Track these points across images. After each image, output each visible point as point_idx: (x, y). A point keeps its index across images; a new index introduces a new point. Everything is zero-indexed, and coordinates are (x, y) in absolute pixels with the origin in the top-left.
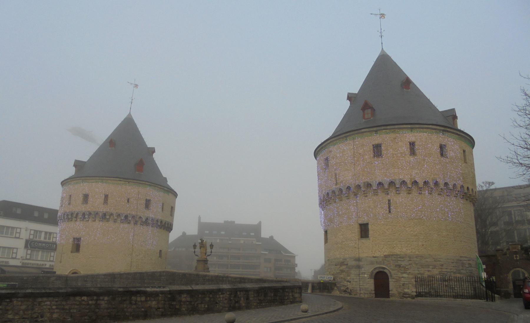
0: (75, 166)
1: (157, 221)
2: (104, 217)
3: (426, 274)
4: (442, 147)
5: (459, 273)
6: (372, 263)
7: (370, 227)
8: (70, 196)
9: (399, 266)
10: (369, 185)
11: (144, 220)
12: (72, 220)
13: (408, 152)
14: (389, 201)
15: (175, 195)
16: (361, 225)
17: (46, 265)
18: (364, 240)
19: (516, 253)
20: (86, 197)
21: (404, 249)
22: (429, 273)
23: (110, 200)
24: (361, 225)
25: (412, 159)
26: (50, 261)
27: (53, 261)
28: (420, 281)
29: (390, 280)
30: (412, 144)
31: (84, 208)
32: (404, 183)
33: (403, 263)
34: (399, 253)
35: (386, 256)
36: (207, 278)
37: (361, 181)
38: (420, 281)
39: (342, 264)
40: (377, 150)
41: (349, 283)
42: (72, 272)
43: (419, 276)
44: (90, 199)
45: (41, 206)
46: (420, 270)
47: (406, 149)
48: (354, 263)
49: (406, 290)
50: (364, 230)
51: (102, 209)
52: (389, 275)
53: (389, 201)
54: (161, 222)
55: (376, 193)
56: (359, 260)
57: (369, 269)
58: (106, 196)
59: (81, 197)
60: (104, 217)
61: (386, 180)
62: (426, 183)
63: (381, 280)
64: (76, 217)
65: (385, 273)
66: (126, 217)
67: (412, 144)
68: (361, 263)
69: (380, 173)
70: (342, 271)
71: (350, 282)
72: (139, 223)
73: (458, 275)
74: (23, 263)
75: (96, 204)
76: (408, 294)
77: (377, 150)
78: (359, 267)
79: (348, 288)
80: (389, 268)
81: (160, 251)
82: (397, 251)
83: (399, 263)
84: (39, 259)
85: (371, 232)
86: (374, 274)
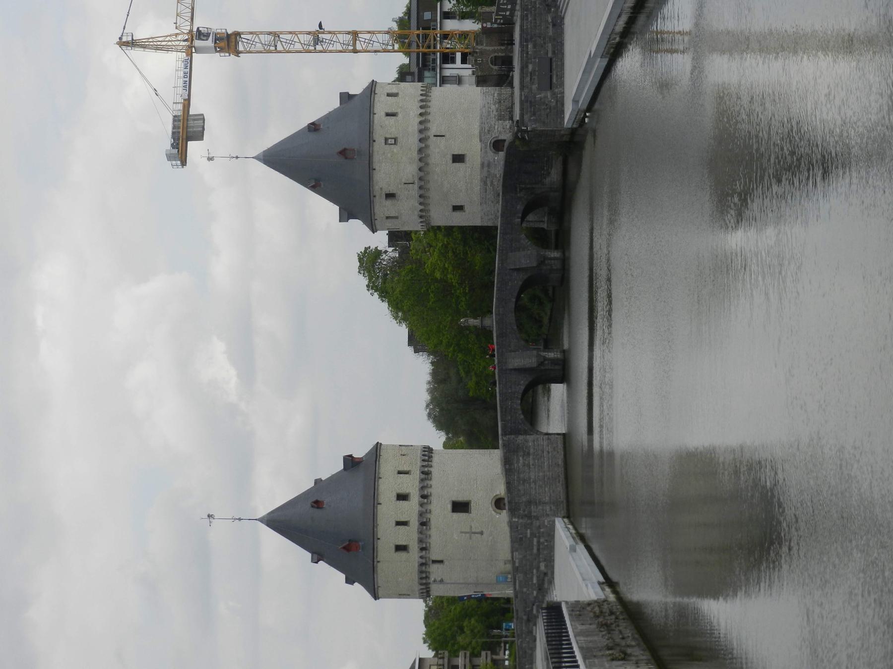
6: (486, 152)
7: (456, 153)
10: (420, 151)
18: (467, 159)
19: (476, 61)
20: (402, 497)
23: (406, 469)
25: (400, 115)
28: (500, 118)
30: (388, 115)
31: (415, 499)
32: (421, 123)
35: (481, 141)
37: (415, 155)
38: (500, 118)
39: (485, 183)
47: (392, 119)
48: (486, 169)
50: (458, 159)
51: (416, 474)
55: (427, 147)
56: (482, 165)
58: (400, 473)
60: (426, 474)
62: (421, 107)
67: (388, 115)
68: (486, 163)
69: (413, 141)
70: (492, 183)
75: (410, 484)
78: (489, 165)
80: (490, 139)
82: (477, 132)
85: (460, 153)
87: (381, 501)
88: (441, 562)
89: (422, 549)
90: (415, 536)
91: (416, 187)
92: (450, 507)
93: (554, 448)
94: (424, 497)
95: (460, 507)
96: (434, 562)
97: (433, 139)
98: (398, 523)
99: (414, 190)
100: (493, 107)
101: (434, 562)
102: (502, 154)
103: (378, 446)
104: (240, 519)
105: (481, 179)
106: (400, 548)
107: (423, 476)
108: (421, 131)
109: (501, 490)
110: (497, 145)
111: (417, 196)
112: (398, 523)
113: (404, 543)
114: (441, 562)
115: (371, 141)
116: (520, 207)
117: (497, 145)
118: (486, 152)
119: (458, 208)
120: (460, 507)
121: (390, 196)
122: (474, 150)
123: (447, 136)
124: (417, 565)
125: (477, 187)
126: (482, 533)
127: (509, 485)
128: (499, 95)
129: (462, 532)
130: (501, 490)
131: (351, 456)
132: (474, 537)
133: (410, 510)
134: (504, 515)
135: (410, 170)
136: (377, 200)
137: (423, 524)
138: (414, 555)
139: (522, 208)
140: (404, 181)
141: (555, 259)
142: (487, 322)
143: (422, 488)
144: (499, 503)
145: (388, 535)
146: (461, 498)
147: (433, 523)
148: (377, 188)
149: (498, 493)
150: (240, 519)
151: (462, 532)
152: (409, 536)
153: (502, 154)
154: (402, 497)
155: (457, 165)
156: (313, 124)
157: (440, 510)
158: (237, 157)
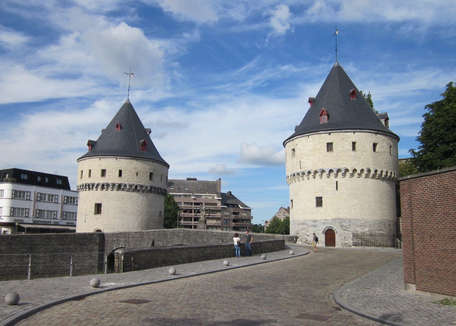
0: (88, 145)
1: (158, 189)
4: (375, 145)
5: (382, 231)
6: (324, 223)
7: (323, 199)
8: (90, 171)
9: (342, 226)
11: (149, 189)
12: (92, 190)
13: (351, 148)
14: (337, 182)
15: (168, 166)
16: (317, 198)
17: (51, 222)
18: (319, 208)
20: (103, 172)
21: (346, 215)
22: (361, 231)
24: (317, 198)
25: (353, 153)
26: (54, 219)
27: (56, 219)
29: (336, 235)
33: (345, 224)
34: (342, 217)
35: (333, 219)
36: (214, 234)
39: (303, 224)
40: (330, 146)
41: (308, 237)
42: (96, 230)
43: (355, 232)
44: (107, 173)
45: (36, 171)
46: (355, 228)
48: (312, 223)
49: (347, 242)
50: (319, 202)
52: (335, 232)
53: (337, 182)
54: (161, 190)
56: (315, 221)
58: (120, 172)
59: (100, 173)
60: (119, 187)
61: (335, 167)
63: (330, 235)
64: (97, 187)
66: (136, 187)
68: (315, 224)
70: (304, 229)
71: (309, 236)
72: (146, 191)
73: (381, 232)
74: (34, 221)
75: (112, 178)
76: (348, 244)
77: (330, 146)
78: (315, 226)
79: (307, 240)
81: (160, 212)
82: (341, 216)
83: (342, 224)
84: (45, 217)
86: (325, 231)
87: (102, 159)
92: (98, 202)
94: (103, 186)
97: (336, 180)
98: (90, 171)
105: (306, 221)
107: (117, 185)
118: (324, 223)
122: (326, 216)
123: (337, 192)
126: (85, 222)
129: (86, 210)
133: (97, 179)
140: (302, 160)
143: (108, 185)
147: (91, 191)
151: (86, 210)
154: (103, 172)
155: (314, 201)
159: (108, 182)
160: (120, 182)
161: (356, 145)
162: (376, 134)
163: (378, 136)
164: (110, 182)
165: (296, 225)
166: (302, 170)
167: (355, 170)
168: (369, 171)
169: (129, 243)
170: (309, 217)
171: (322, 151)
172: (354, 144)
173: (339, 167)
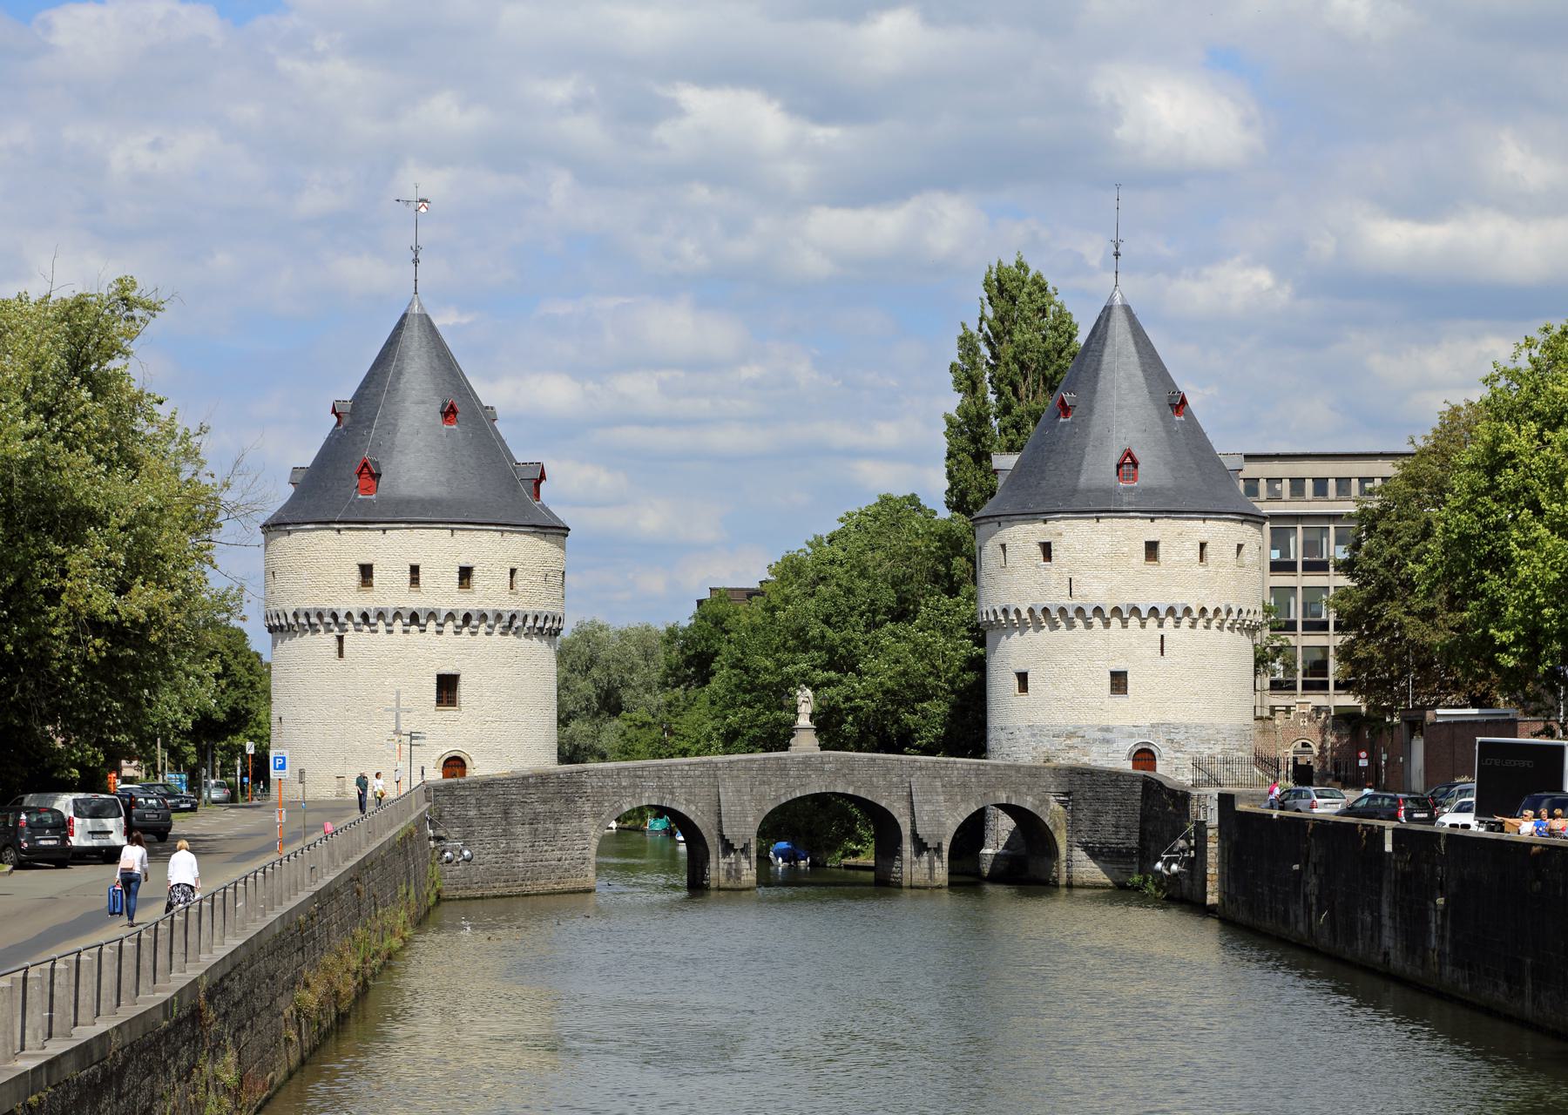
2: (510, 624)
3: (1207, 752)
7: (1129, 677)
9: (1172, 741)
16: (1113, 674)
18: (1119, 699)
20: (465, 574)
21: (1180, 716)
23: (520, 583)
24: (1113, 674)
25: (1202, 570)
31: (465, 602)
33: (1177, 737)
35: (1152, 726)
37: (1124, 601)
39: (1070, 735)
40: (1152, 549)
48: (1099, 735)
50: (1119, 681)
51: (508, 605)
56: (1107, 729)
57: (1127, 746)
58: (513, 571)
60: (510, 624)
65: (1152, 753)
68: (1108, 736)
69: (1151, 588)
70: (1071, 747)
75: (488, 594)
77: (1152, 549)
78: (1107, 741)
82: (1170, 718)
88: (341, 654)
89: (365, 616)
90: (390, 604)
91: (1065, 601)
92: (448, 670)
93: (567, 870)
94: (467, 618)
95: (447, 687)
96: (340, 639)
97: (1160, 631)
98: (415, 570)
99: (1057, 597)
100: (1218, 749)
101: (340, 639)
102: (1127, 766)
103: (563, 531)
104: (416, 261)
106: (366, 571)
107: (506, 617)
108: (1171, 611)
109: (479, 769)
110: (1145, 756)
111: (1045, 603)
112: (415, 570)
113: (375, 581)
114: (341, 654)
115: (1154, 514)
116: (1028, 803)
117: (1145, 756)
118: (1131, 736)
119: (1023, 678)
120: (447, 687)
121: (1046, 549)
123: (1162, 661)
124: (335, 607)
125: (1062, 718)
127: (487, 784)
128: (1240, 761)
129: (398, 693)
130: (479, 769)
131: (543, 477)
132: (391, 717)
133: (440, 592)
134: (435, 775)
135: (1095, 592)
136: (1040, 526)
137: (414, 618)
138: (353, 600)
139: (1028, 806)
140: (1075, 577)
141: (931, 868)
142: (805, 742)
143: (483, 617)
144: (454, 765)
145: (391, 548)
146: (464, 690)
148: (1062, 525)
149: (476, 763)
150: (416, 261)
151: (398, 693)
152: (391, 592)
153: (1127, 766)
154: (465, 574)
156: (1184, 402)
157: (441, 650)
158: (1117, 255)
159: (481, 607)
160: (514, 608)
161: (1208, 549)
162: (1242, 522)
163: (1246, 526)
164: (489, 607)
165: (1045, 739)
166: (1077, 602)
167: (1203, 611)
168: (1229, 611)
169: (672, 793)
170: (1087, 719)
171: (1134, 561)
172: (1203, 546)
173: (1170, 603)
